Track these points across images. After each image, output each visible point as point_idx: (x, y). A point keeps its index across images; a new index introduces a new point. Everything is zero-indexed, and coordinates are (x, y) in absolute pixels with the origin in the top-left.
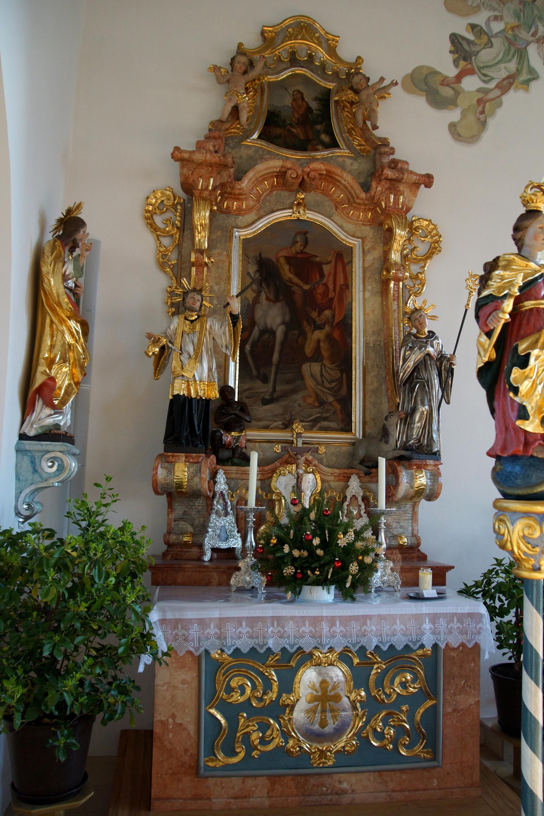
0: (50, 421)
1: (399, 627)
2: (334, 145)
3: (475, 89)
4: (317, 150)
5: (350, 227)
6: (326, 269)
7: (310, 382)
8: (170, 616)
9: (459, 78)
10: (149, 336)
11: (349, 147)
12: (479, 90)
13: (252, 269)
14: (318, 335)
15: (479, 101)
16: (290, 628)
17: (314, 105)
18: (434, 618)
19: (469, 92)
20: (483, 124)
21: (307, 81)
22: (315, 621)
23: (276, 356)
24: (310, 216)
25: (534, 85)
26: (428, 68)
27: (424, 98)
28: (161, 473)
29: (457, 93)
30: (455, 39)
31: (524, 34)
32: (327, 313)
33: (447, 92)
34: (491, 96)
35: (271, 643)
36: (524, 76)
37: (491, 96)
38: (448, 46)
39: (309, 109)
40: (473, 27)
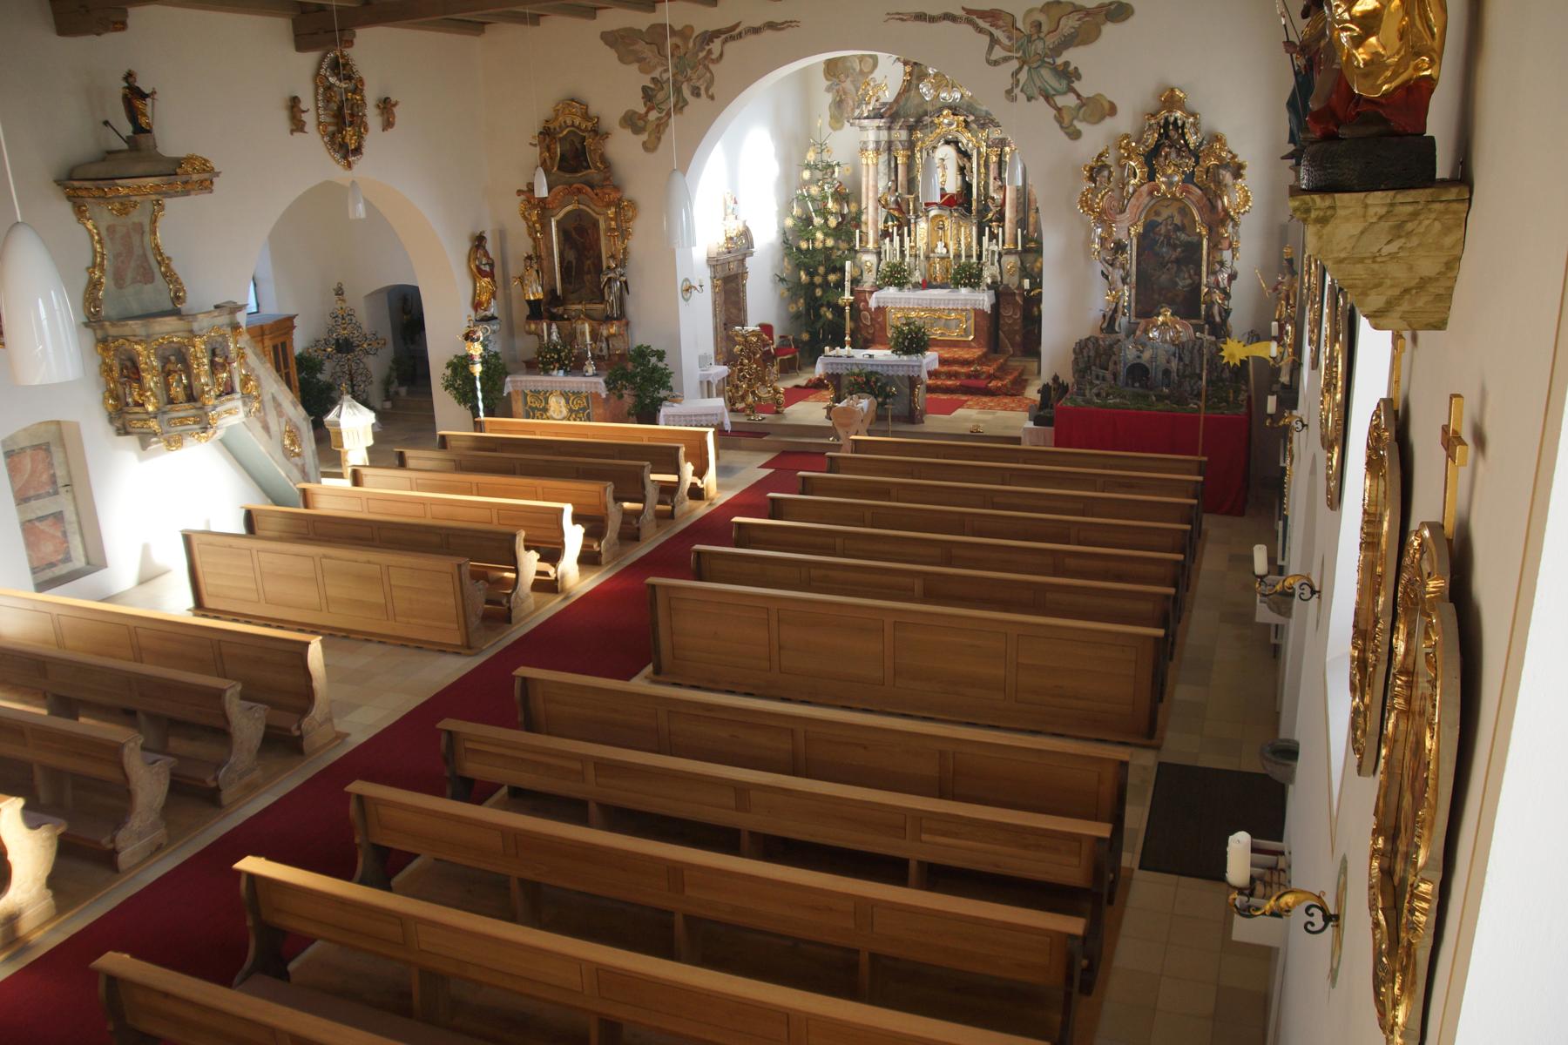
0: (483, 314)
1: (575, 385)
2: (589, 167)
3: (654, 119)
4: (581, 171)
5: (597, 209)
6: (589, 231)
7: (588, 284)
8: (513, 379)
9: (647, 113)
10: (514, 277)
11: (597, 168)
12: (658, 119)
13: (561, 234)
14: (589, 262)
15: (658, 126)
16: (545, 384)
17: (579, 146)
18: (586, 383)
19: (652, 121)
20: (659, 139)
21: (575, 132)
22: (551, 382)
23: (574, 273)
24: (581, 206)
25: (686, 109)
26: (632, 110)
27: (630, 130)
28: (527, 327)
29: (646, 122)
30: (645, 89)
31: (680, 78)
32: (591, 252)
33: (641, 123)
34: (664, 120)
35: (540, 388)
36: (680, 105)
37: (664, 120)
38: (641, 94)
39: (577, 149)
40: (653, 79)
